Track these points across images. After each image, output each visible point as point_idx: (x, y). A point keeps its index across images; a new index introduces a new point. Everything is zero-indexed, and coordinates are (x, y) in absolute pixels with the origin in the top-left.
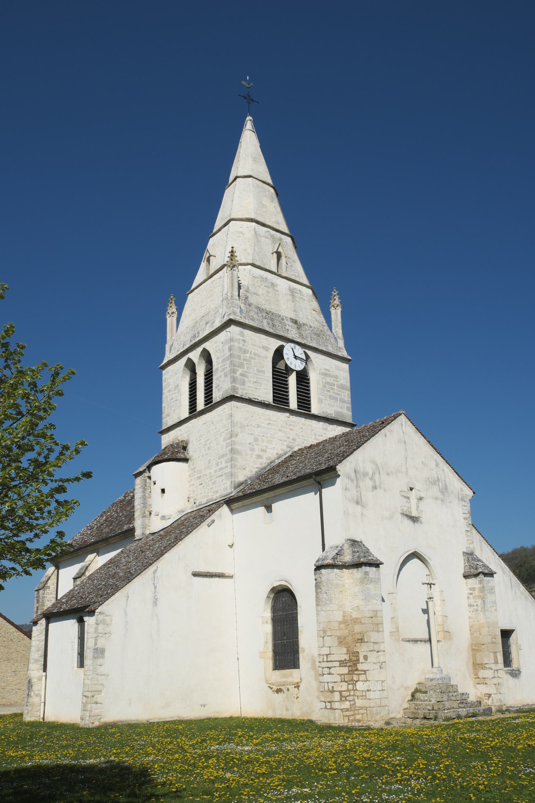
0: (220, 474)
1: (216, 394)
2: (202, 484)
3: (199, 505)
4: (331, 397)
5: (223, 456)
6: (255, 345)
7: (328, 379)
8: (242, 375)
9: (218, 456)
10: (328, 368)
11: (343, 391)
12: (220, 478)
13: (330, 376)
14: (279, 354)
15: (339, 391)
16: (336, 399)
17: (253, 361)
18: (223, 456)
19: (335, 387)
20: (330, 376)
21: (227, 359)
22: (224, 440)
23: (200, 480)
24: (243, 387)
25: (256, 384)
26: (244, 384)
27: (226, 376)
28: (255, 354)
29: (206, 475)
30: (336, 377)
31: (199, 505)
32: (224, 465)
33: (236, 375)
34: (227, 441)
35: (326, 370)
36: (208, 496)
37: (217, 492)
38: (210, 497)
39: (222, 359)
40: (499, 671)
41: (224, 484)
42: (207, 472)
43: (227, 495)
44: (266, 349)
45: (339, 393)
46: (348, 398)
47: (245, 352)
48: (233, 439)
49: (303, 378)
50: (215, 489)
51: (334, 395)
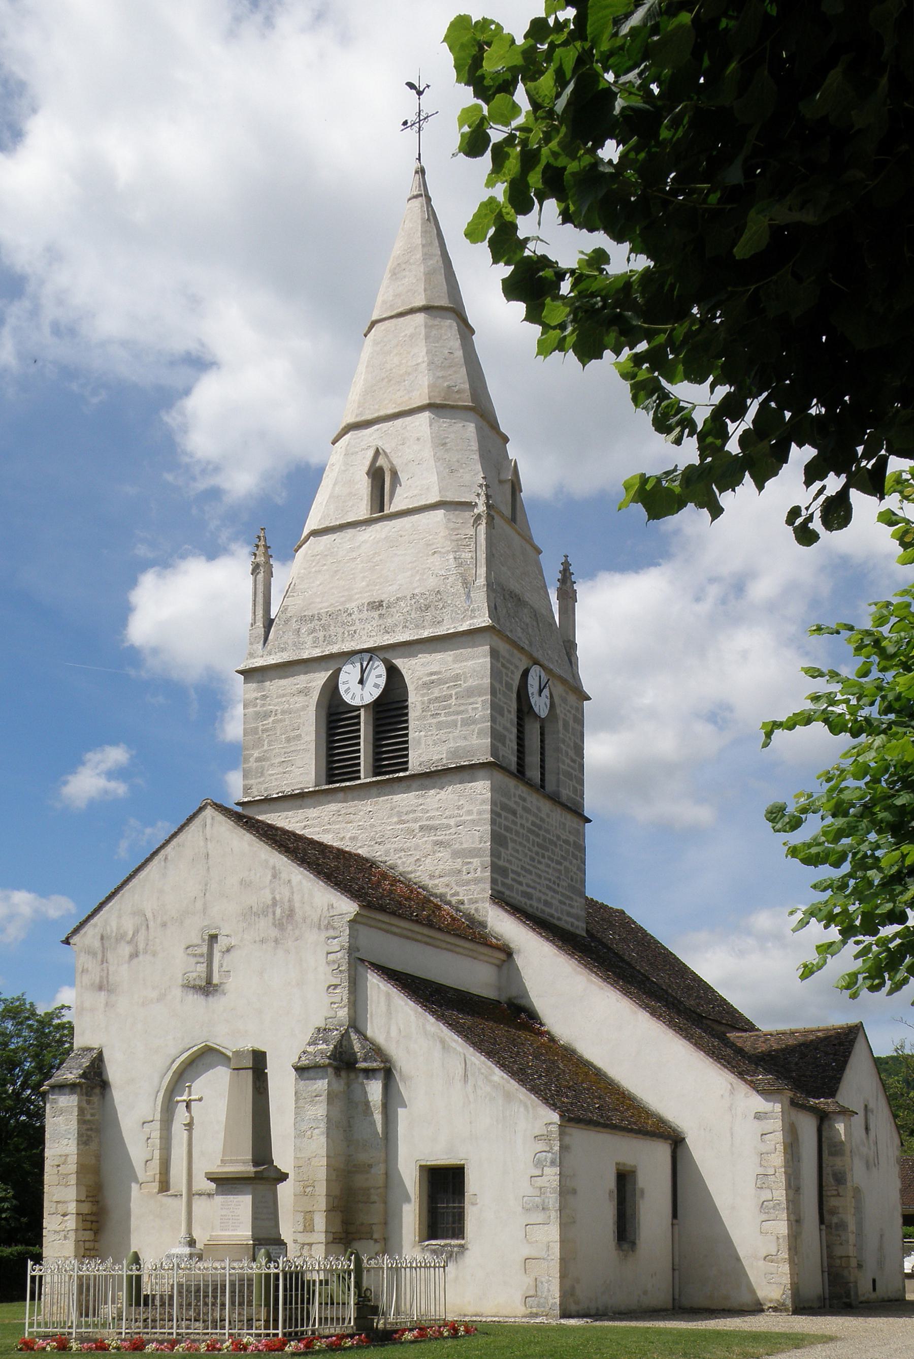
4: (440, 726)
6: (284, 696)
7: (436, 692)
8: (258, 760)
10: (435, 669)
11: (471, 700)
13: (441, 682)
14: (331, 690)
15: (460, 705)
16: (454, 724)
17: (279, 726)
19: (453, 701)
20: (441, 682)
24: (262, 779)
25: (285, 765)
26: (262, 774)
28: (283, 712)
30: (457, 677)
33: (250, 764)
35: (432, 674)
40: (314, 1247)
44: (305, 692)
45: (462, 708)
46: (483, 709)
47: (267, 715)
49: (391, 709)
51: (449, 718)
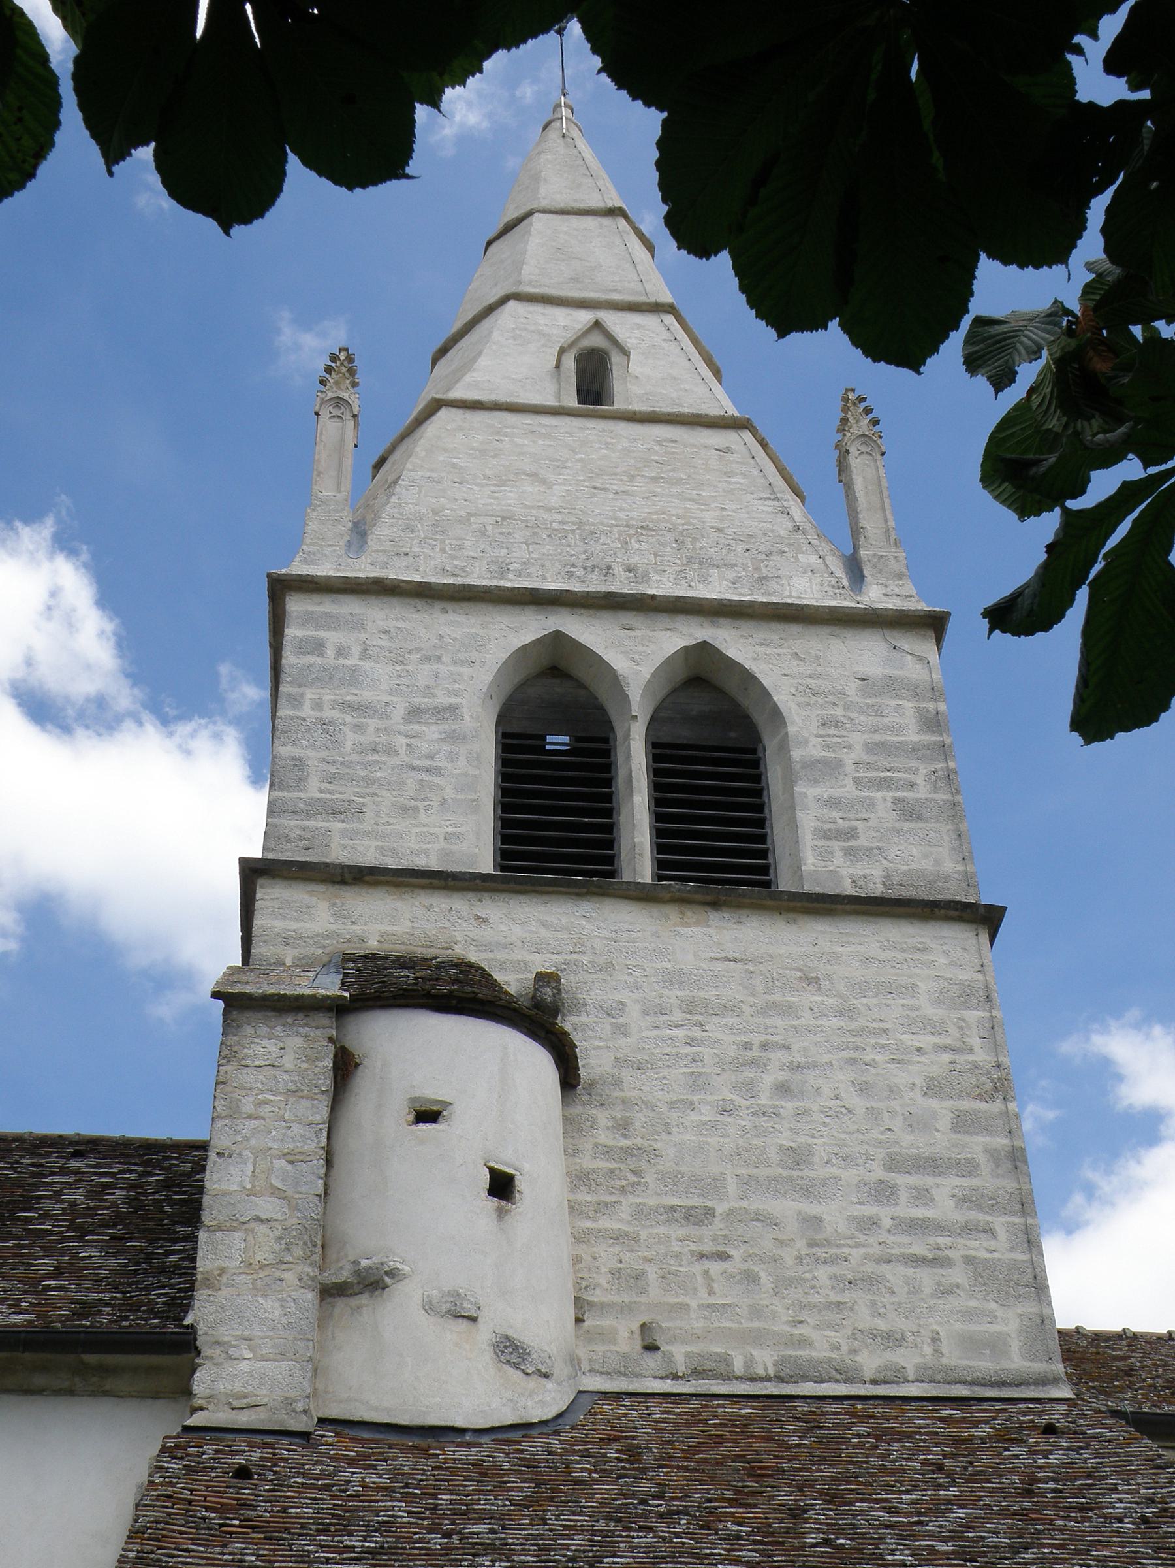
0: (919, 1249)
1: (825, 855)
2: (723, 1256)
3: (697, 1373)
5: (932, 1165)
9: (880, 1153)
12: (927, 1278)
18: (932, 1165)
21: (915, 750)
22: (933, 1088)
23: (706, 1232)
27: (909, 811)
29: (773, 1223)
31: (697, 1373)
32: (944, 1208)
34: (966, 1104)
36: (804, 1342)
37: (893, 1340)
38: (820, 1351)
39: (868, 737)
41: (968, 1315)
42: (786, 1207)
43: (1002, 1384)
48: (1012, 1106)
50: (865, 1319)
